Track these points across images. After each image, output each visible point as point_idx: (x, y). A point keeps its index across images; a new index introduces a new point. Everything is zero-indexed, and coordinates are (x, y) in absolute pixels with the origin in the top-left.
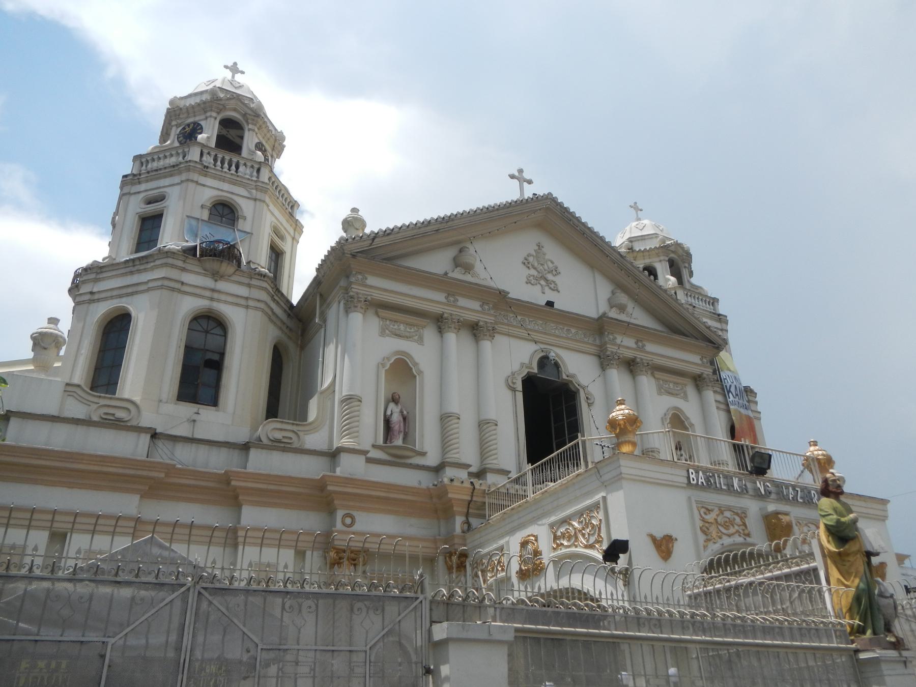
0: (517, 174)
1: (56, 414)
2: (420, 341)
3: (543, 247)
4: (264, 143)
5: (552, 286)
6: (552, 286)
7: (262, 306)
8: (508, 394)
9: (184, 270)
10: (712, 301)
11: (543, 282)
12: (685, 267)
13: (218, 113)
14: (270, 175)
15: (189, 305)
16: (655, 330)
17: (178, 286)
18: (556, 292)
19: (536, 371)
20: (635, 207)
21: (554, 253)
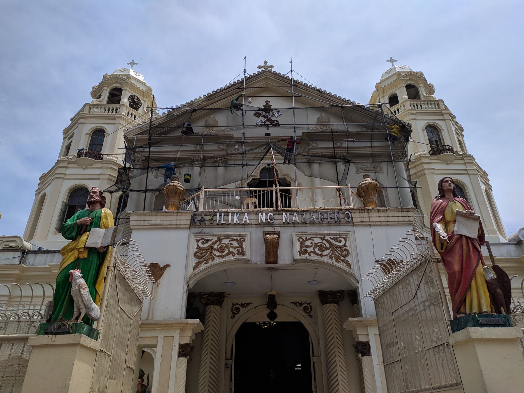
0: (263, 64)
3: (269, 102)
7: (108, 176)
9: (67, 167)
10: (436, 103)
11: (268, 123)
12: (420, 87)
13: (108, 87)
14: (128, 110)
15: (68, 185)
16: (357, 132)
17: (63, 176)
19: (258, 177)
20: (392, 61)
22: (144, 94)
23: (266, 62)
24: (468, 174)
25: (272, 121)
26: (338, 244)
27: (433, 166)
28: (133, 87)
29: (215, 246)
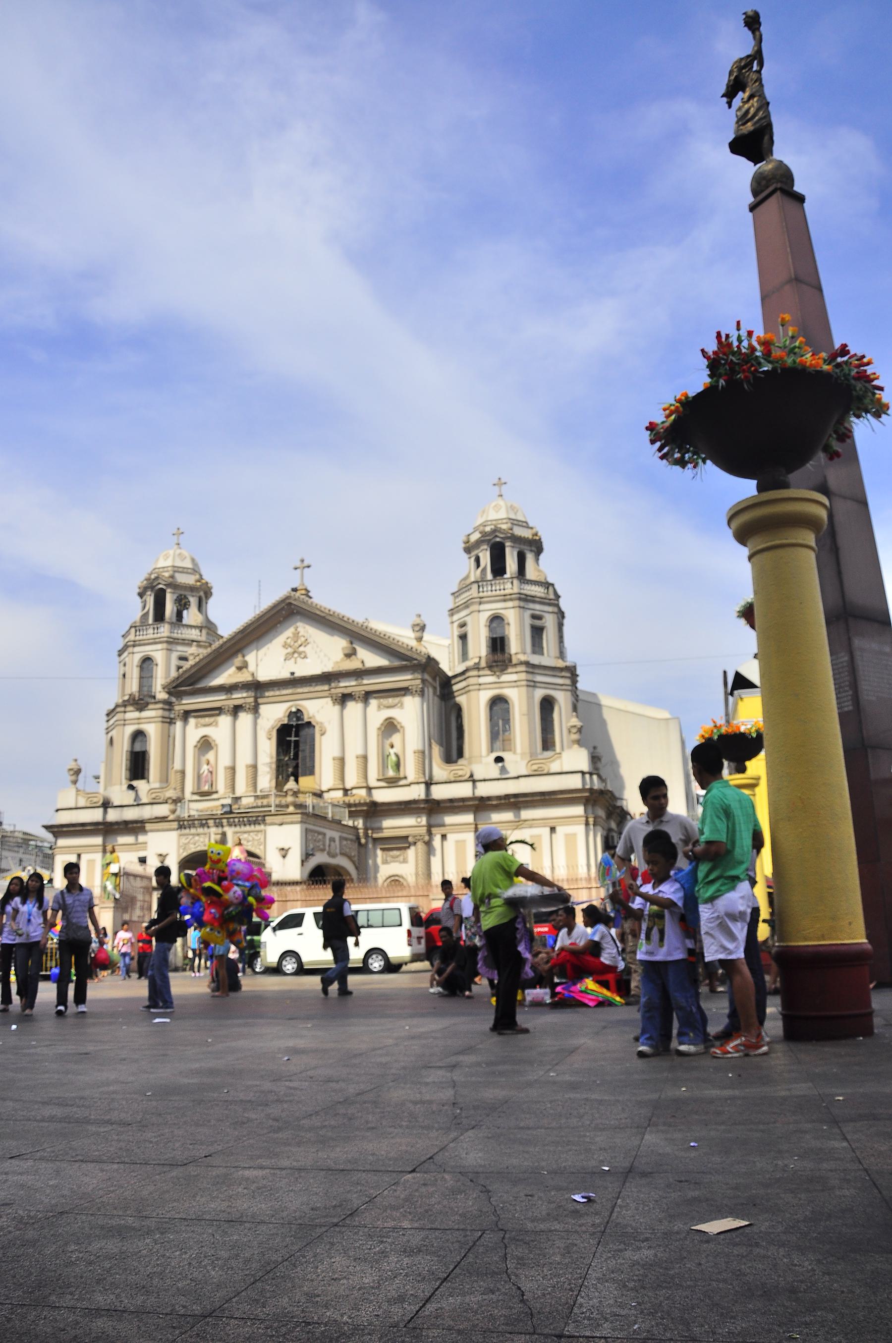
0: (298, 564)
1: (73, 806)
2: (217, 725)
4: (183, 593)
5: (302, 656)
6: (302, 656)
7: (160, 719)
8: (268, 741)
10: (510, 580)
11: (296, 655)
13: (152, 591)
15: (130, 729)
17: (122, 722)
18: (305, 659)
19: (286, 722)
21: (306, 630)
22: (192, 589)
23: (302, 561)
24: (517, 686)
25: (300, 653)
26: (256, 838)
27: (482, 680)
28: (174, 586)
29: (192, 841)
